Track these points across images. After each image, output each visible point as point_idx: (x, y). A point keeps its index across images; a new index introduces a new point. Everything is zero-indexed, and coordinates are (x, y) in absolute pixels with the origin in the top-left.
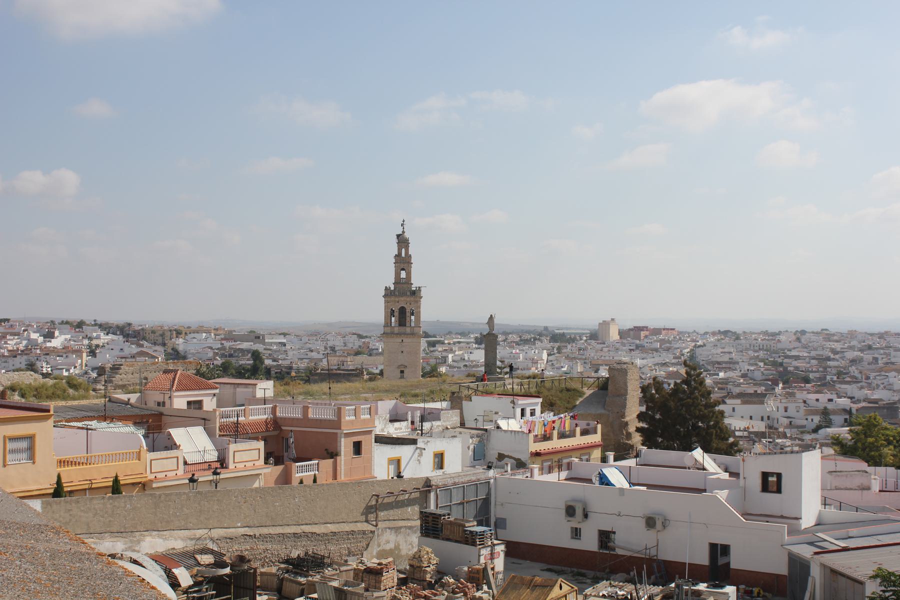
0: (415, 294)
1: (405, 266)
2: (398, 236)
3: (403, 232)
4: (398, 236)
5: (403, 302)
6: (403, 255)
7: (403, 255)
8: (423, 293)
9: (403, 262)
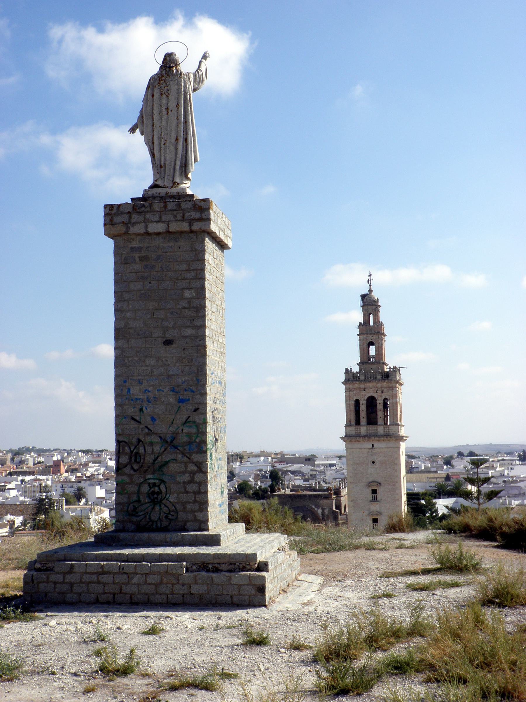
0: (390, 377)
2: (363, 297)
3: (370, 291)
4: (363, 297)
5: (371, 389)
6: (371, 323)
7: (371, 323)
8: (404, 376)
9: (371, 333)
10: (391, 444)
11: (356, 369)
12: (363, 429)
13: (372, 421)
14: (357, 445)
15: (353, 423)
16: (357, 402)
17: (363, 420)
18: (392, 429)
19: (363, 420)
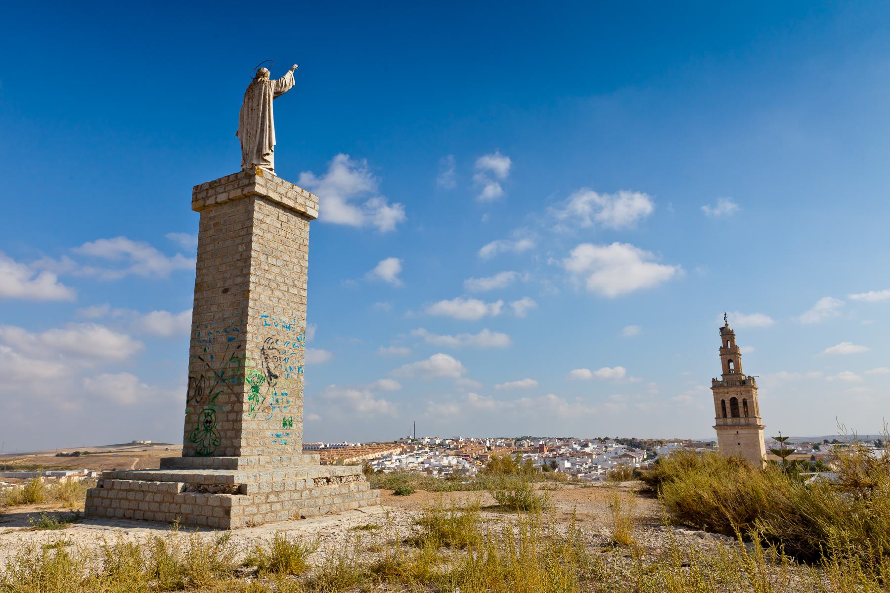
0: (747, 384)
1: (731, 357)
2: (722, 329)
4: (722, 329)
5: (732, 393)
9: (729, 353)
10: (752, 431)
11: (720, 379)
12: (729, 421)
13: (735, 414)
14: (726, 432)
15: (721, 416)
16: (723, 401)
17: (729, 415)
18: (751, 420)
19: (729, 415)
